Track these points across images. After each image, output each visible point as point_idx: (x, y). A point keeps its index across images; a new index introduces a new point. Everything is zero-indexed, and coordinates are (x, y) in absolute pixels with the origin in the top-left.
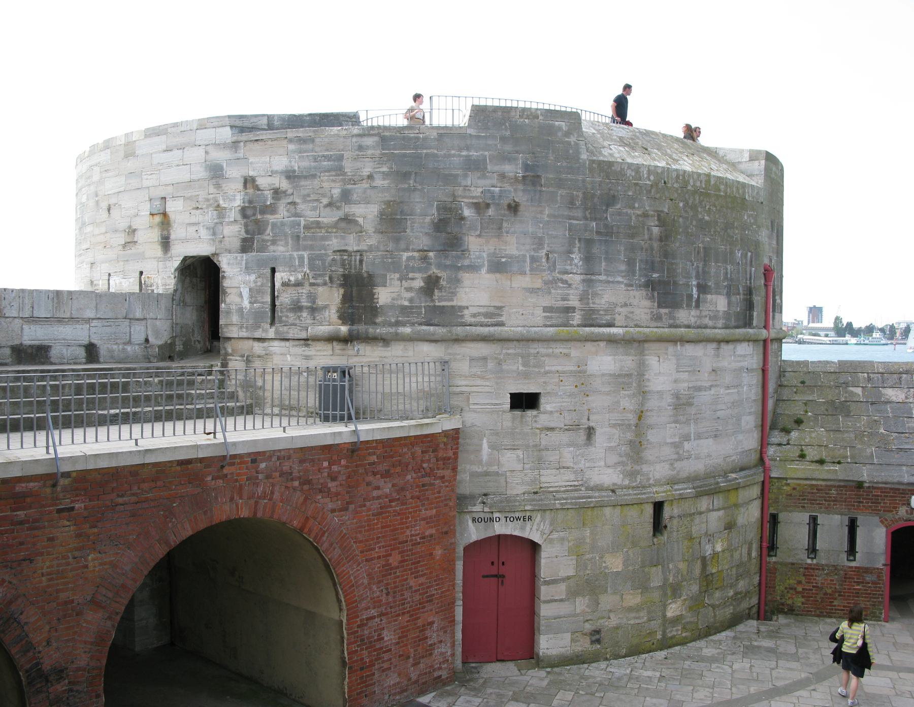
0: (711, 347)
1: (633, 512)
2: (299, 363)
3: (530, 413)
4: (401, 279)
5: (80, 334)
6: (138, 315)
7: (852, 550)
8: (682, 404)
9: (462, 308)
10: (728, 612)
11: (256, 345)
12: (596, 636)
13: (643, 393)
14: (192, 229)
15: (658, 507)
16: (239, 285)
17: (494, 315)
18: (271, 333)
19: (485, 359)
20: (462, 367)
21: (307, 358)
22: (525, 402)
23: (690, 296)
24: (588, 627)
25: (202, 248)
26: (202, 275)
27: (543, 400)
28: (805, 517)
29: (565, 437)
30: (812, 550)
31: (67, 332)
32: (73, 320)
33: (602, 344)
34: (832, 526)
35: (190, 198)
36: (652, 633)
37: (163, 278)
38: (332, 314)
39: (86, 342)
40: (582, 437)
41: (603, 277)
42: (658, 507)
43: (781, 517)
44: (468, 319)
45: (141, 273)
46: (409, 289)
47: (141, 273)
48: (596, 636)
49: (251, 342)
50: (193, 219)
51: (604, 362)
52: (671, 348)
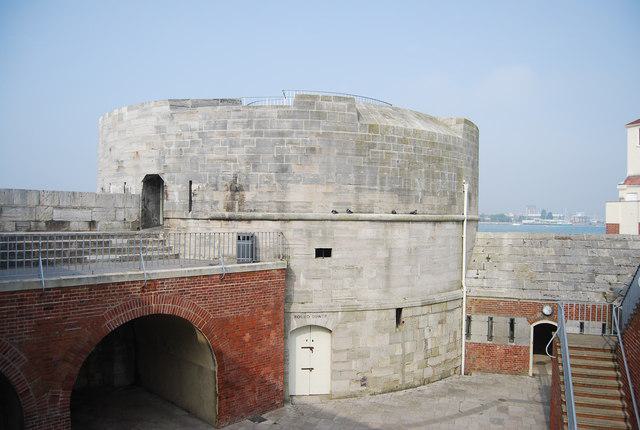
0: (430, 225)
1: (384, 314)
3: (327, 259)
5: (87, 215)
7: (512, 337)
8: (413, 253)
9: (289, 203)
10: (440, 370)
11: (182, 221)
12: (364, 382)
13: (390, 250)
14: (150, 160)
15: (399, 311)
16: (175, 194)
17: (307, 205)
18: (190, 215)
19: (301, 230)
20: (289, 234)
22: (323, 253)
23: (417, 197)
24: (360, 377)
25: (154, 171)
26: (154, 183)
27: (333, 253)
28: (485, 317)
29: (348, 272)
30: (490, 337)
31: (78, 214)
32: (83, 208)
33: (367, 223)
34: (501, 323)
36: (396, 381)
37: (137, 188)
38: (221, 206)
40: (356, 271)
42: (399, 311)
43: (473, 317)
44: (293, 209)
48: (364, 382)
51: (368, 231)
52: (405, 224)
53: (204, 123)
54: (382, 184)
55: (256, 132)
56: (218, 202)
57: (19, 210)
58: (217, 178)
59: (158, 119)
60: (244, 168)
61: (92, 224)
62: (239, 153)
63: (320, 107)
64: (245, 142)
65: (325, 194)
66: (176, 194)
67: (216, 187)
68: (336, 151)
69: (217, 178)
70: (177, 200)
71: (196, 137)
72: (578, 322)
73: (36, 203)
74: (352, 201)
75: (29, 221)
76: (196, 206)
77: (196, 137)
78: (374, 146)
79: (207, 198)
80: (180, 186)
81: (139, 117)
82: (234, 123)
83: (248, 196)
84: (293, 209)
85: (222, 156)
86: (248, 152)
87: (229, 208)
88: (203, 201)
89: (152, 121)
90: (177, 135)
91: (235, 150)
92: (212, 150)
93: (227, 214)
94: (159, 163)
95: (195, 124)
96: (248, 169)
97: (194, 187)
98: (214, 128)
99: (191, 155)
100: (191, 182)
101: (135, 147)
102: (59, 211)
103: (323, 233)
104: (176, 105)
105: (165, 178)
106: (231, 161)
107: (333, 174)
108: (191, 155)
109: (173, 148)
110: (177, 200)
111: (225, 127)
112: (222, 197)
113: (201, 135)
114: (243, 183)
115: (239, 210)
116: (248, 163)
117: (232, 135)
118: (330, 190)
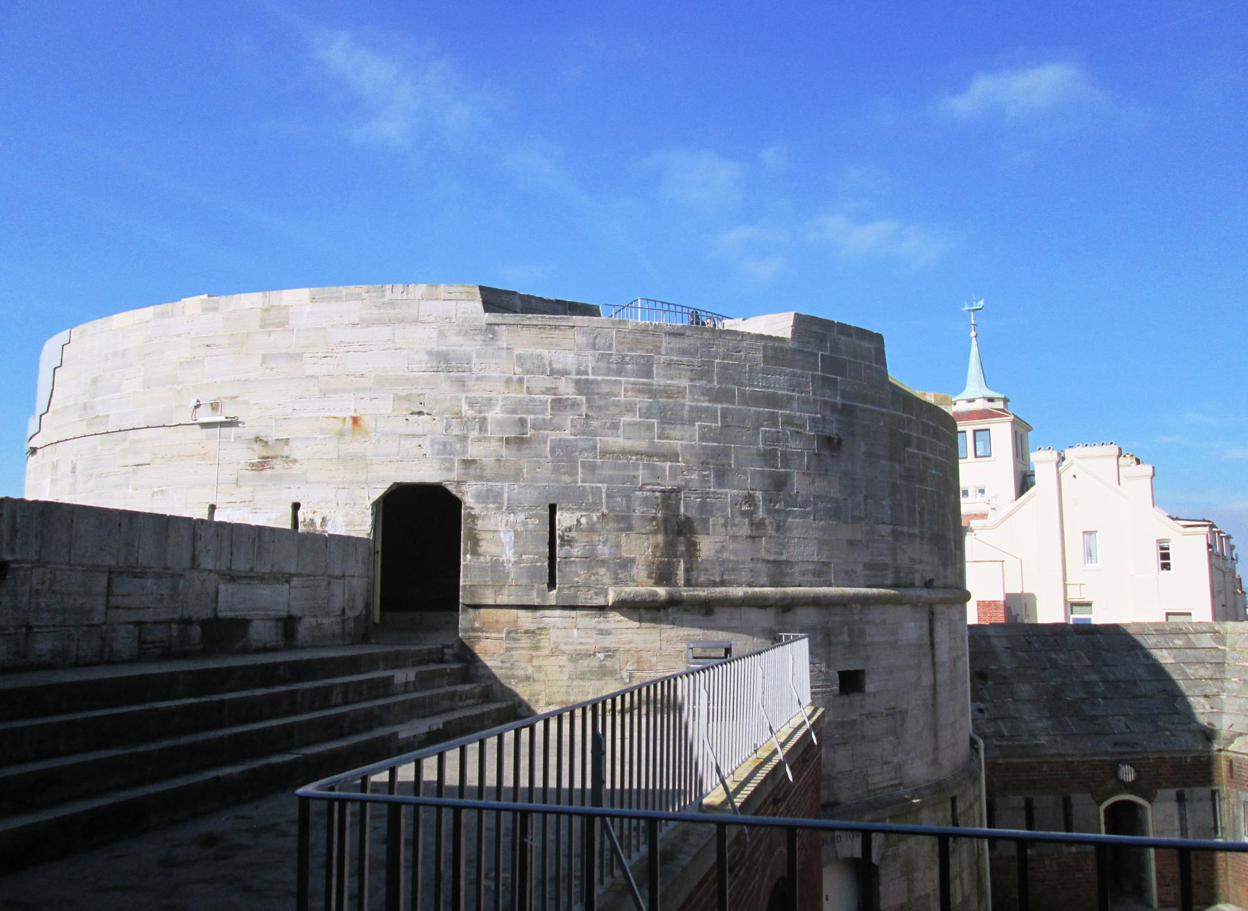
2: (592, 642)
4: (725, 525)
6: (338, 572)
14: (411, 444)
18: (552, 597)
21: (602, 632)
35: (408, 398)
38: (640, 571)
39: (284, 614)
41: (905, 529)
43: (998, 800)
44: (798, 578)
45: (296, 506)
46: (734, 538)
47: (296, 506)
49: (514, 611)
50: (412, 429)
53: (590, 360)
54: (922, 524)
55: (720, 391)
56: (633, 560)
57: (150, 582)
58: (628, 498)
59: (442, 334)
60: (695, 476)
61: (289, 624)
62: (684, 439)
63: (835, 348)
64: (697, 414)
65: (851, 543)
66: (507, 537)
67: (624, 523)
68: (863, 449)
69: (628, 498)
70: (508, 555)
71: (567, 389)
72: (1172, 793)
73: (186, 562)
74: (887, 559)
75: (168, 622)
76: (573, 573)
77: (567, 389)
78: (907, 441)
79: (603, 551)
80: (521, 517)
81: (367, 323)
82: (669, 364)
83: (707, 546)
84: (798, 578)
85: (642, 445)
86: (703, 438)
87: (664, 576)
88: (591, 560)
89: (420, 339)
90: (508, 381)
91: (677, 431)
92: (615, 426)
93: (662, 592)
94: (445, 449)
95: (567, 359)
96: (704, 480)
97: (564, 519)
98: (619, 372)
99: (553, 435)
100: (553, 509)
101: (346, 406)
102: (231, 587)
103: (851, 634)
104: (495, 300)
105: (469, 497)
106: (664, 456)
107: (860, 498)
108: (553, 435)
109: (495, 414)
110: (508, 555)
111: (649, 374)
112: (641, 548)
113: (583, 386)
114: (693, 514)
115: (688, 583)
116: (704, 464)
117: (667, 392)
118: (859, 536)
